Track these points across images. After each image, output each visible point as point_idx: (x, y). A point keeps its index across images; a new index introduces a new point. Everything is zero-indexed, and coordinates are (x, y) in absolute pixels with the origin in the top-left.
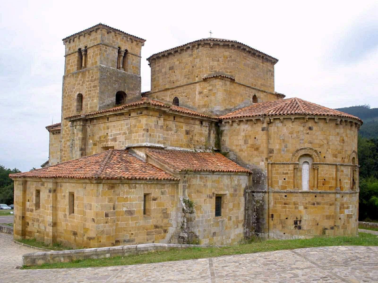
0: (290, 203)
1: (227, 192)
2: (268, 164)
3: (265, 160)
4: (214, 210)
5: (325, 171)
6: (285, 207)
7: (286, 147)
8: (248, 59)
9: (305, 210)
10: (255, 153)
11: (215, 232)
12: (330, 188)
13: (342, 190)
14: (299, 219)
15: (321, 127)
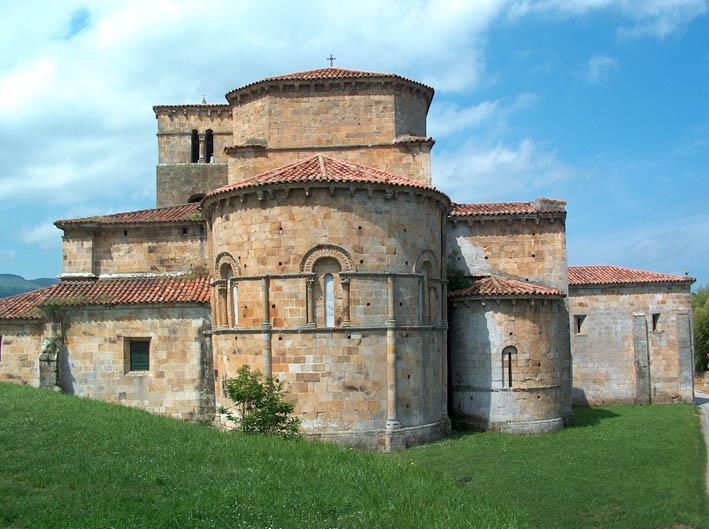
1: (151, 334)
8: (306, 99)
12: (255, 321)
13: (281, 325)
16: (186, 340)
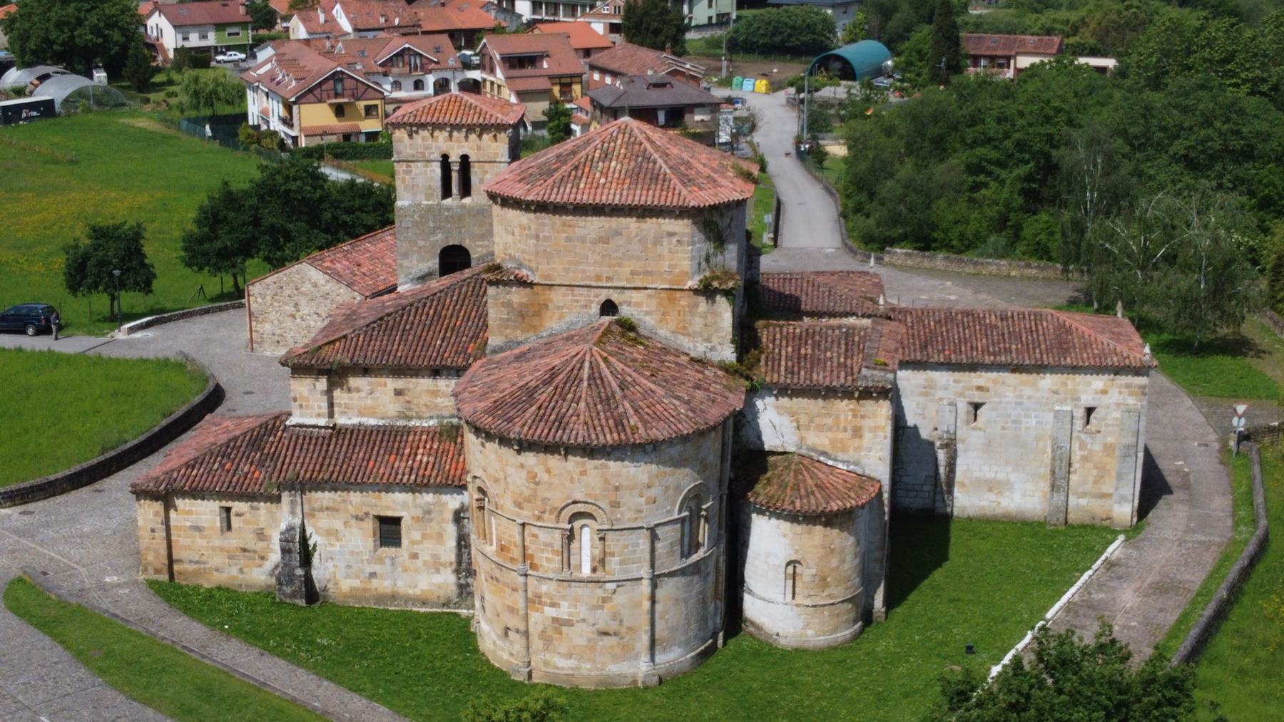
16: (443, 521)
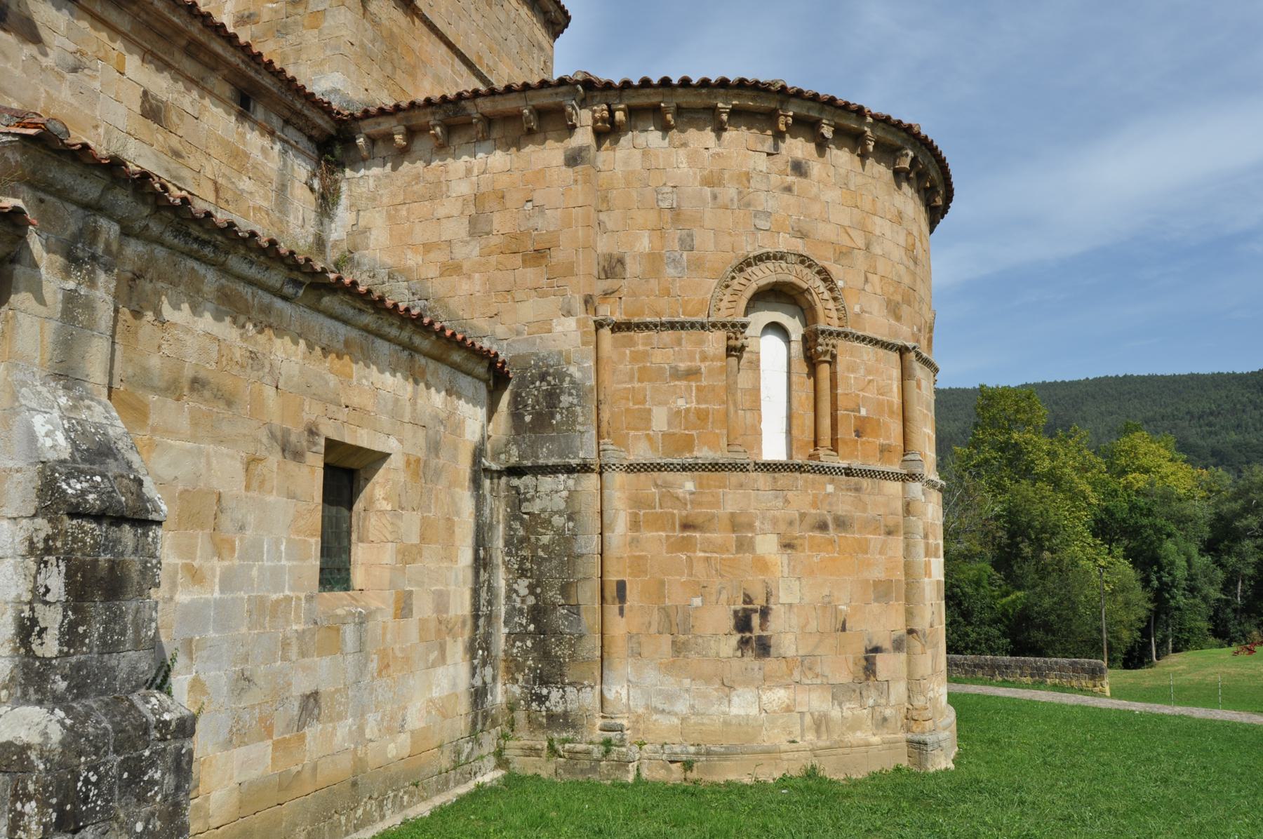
0: (712, 518)
2: (599, 325)
3: (578, 306)
4: (315, 543)
5: (862, 371)
6: (686, 545)
7: (687, 244)
9: (785, 557)
10: (531, 275)
11: (315, 695)
14: (759, 603)
15: (843, 171)
